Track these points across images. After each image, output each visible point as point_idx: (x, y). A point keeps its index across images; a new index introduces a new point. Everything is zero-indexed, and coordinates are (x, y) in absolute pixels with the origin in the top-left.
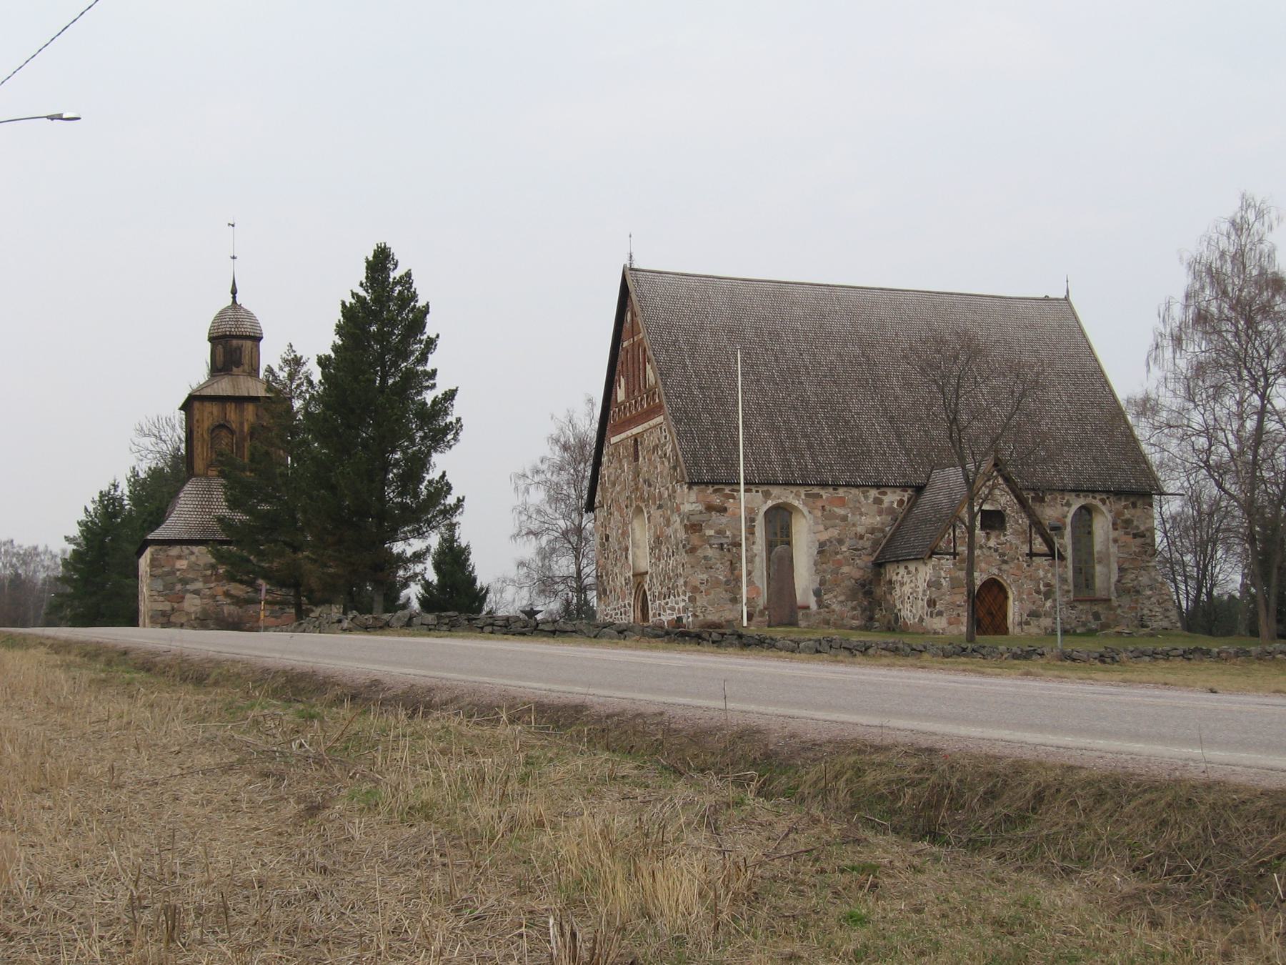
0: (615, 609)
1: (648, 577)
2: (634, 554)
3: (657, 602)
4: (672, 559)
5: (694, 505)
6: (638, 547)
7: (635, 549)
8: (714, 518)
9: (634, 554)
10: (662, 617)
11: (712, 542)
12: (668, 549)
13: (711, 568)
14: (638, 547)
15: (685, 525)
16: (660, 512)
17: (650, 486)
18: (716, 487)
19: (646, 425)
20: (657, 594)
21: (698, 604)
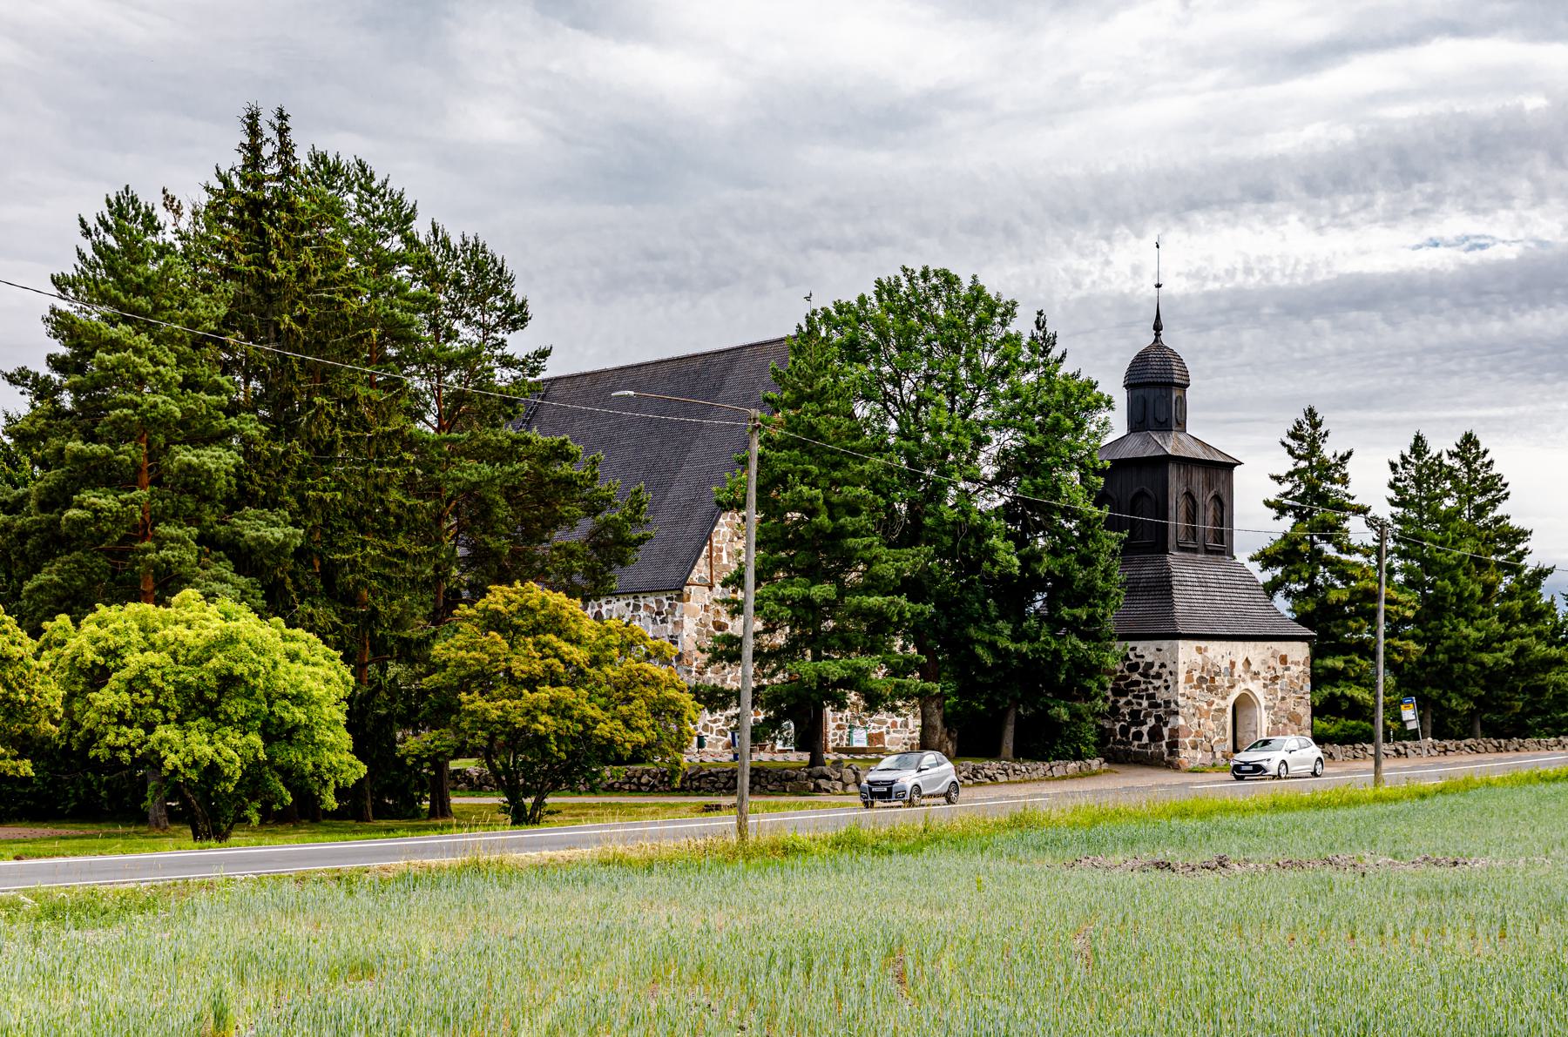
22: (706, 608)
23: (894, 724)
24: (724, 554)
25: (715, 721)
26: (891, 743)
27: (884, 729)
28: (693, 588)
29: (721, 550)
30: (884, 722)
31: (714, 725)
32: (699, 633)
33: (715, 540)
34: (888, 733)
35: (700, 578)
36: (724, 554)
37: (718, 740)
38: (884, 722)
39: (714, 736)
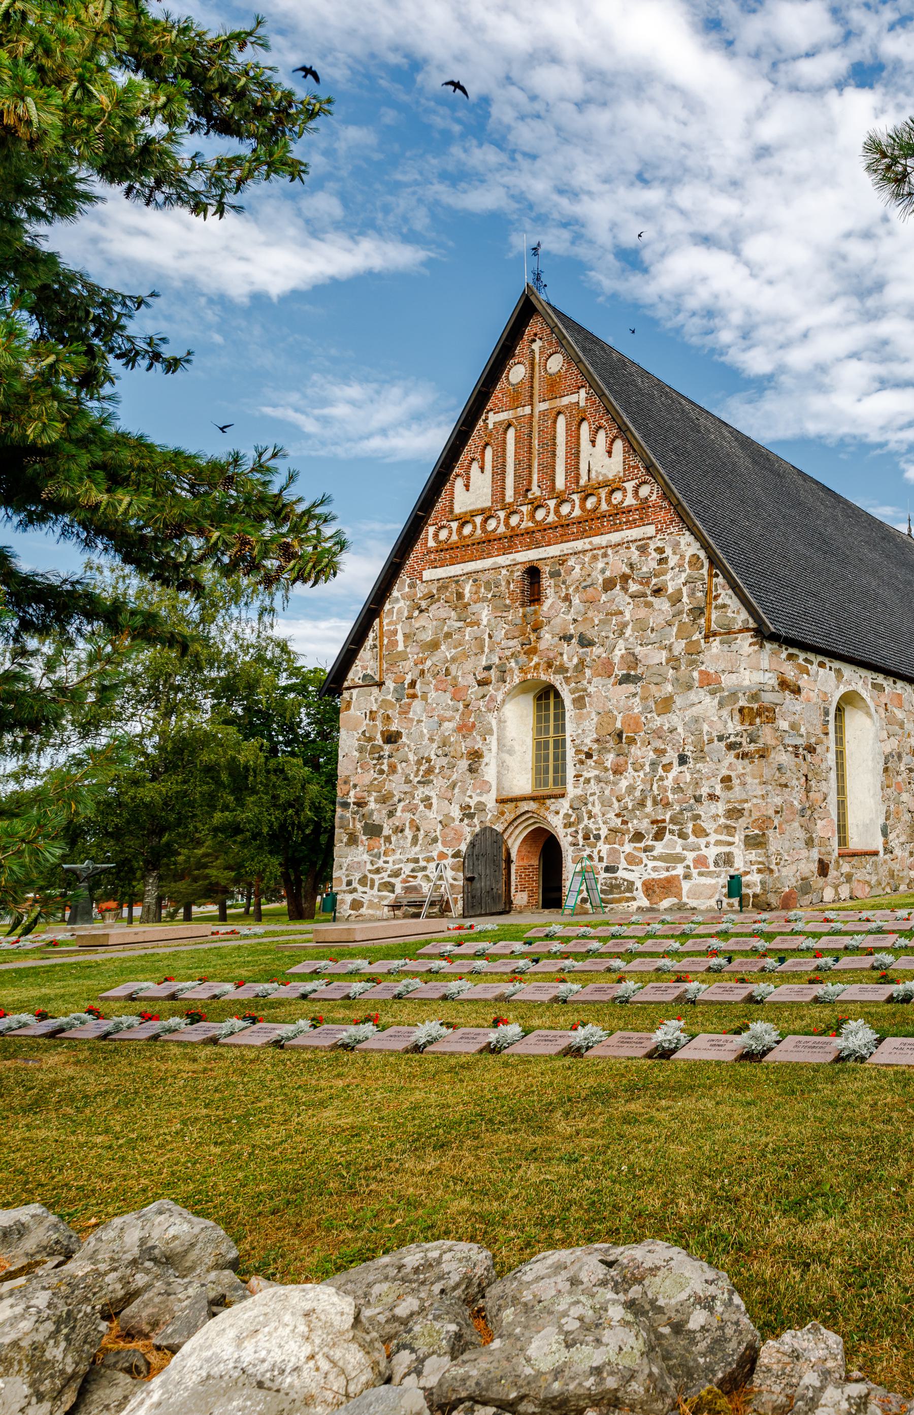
0: (416, 861)
1: (564, 805)
2: (502, 766)
3: (603, 848)
4: (676, 768)
5: (768, 675)
6: (511, 752)
7: (506, 756)
8: (787, 701)
9: (502, 765)
10: (621, 874)
11: (788, 741)
12: (660, 752)
13: (786, 786)
14: (511, 752)
15: (741, 710)
16: (631, 688)
17: (585, 642)
18: (791, 651)
19: (579, 545)
20: (604, 832)
21: (772, 849)
22: (372, 715)
23: (701, 861)
24: (400, 637)
25: (377, 871)
26: (693, 894)
27: (680, 870)
28: (355, 692)
29: (395, 632)
30: (680, 859)
31: (376, 877)
32: (361, 750)
33: (386, 621)
34: (687, 877)
35: (365, 676)
36: (400, 637)
37: (382, 898)
38: (680, 859)
39: (375, 891)
